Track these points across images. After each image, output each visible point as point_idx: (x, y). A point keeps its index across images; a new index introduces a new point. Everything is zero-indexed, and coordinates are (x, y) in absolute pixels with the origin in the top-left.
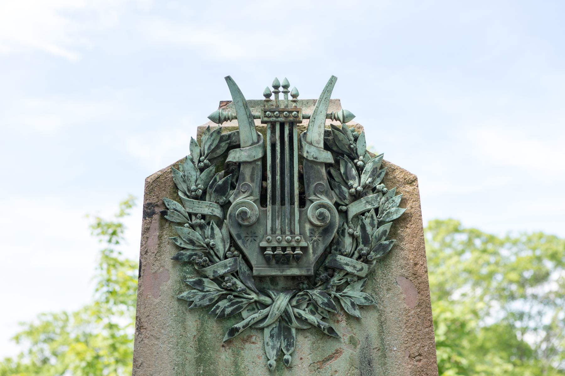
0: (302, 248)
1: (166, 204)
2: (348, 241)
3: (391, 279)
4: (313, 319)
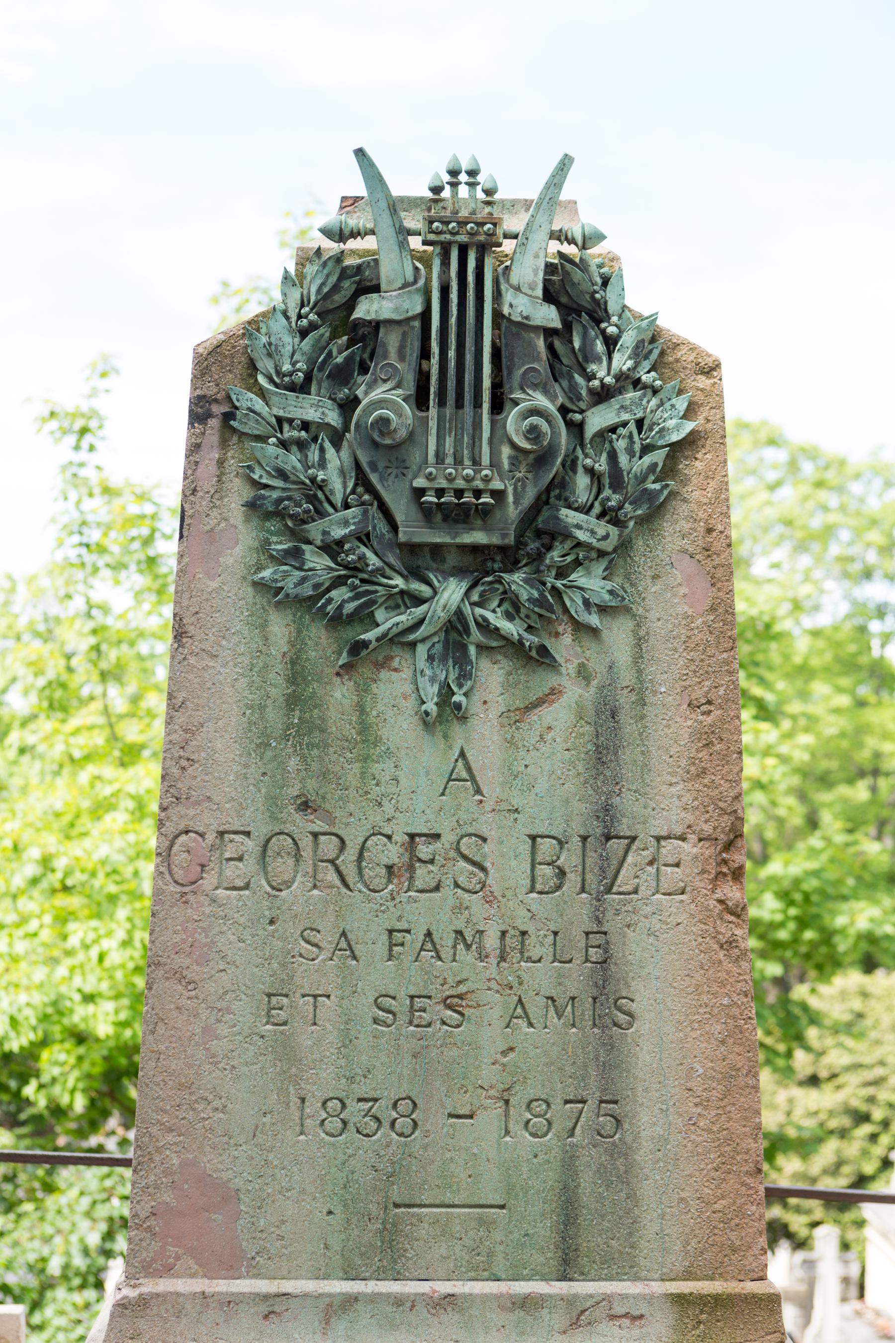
1: (234, 397)
2: (582, 481)
3: (662, 556)
4: (510, 628)
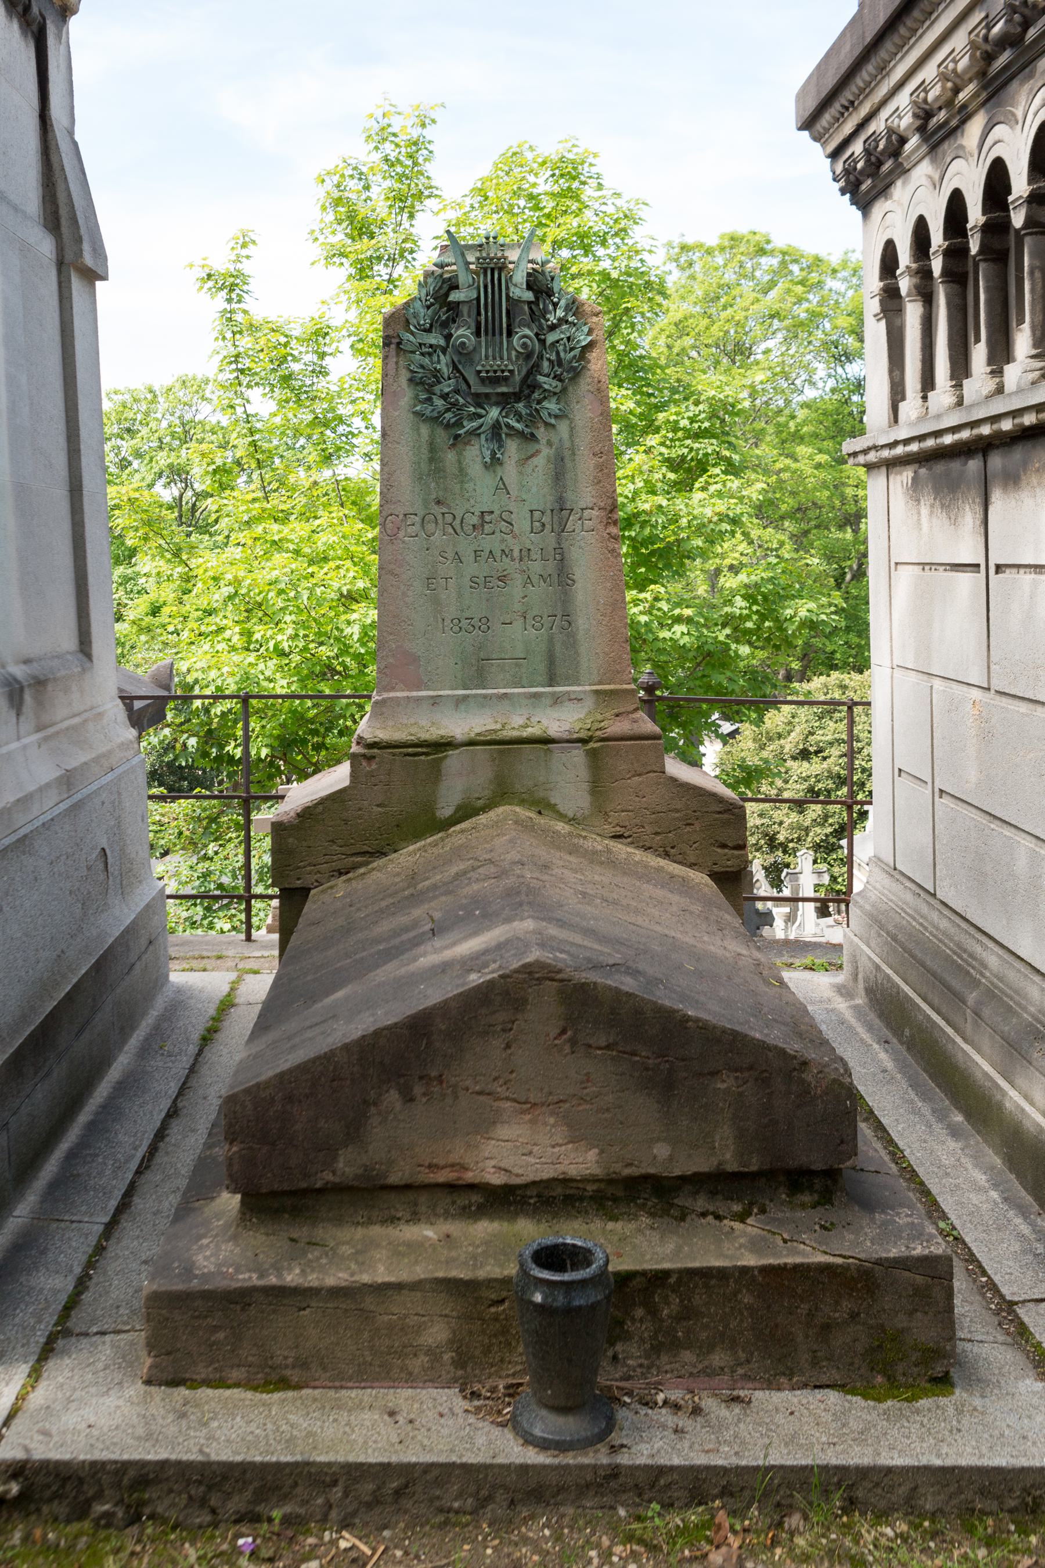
0: (511, 372)
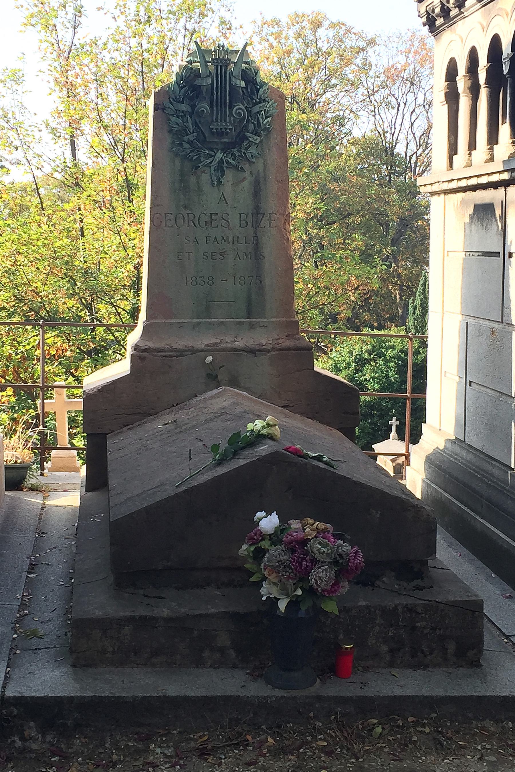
0: (229, 129)
